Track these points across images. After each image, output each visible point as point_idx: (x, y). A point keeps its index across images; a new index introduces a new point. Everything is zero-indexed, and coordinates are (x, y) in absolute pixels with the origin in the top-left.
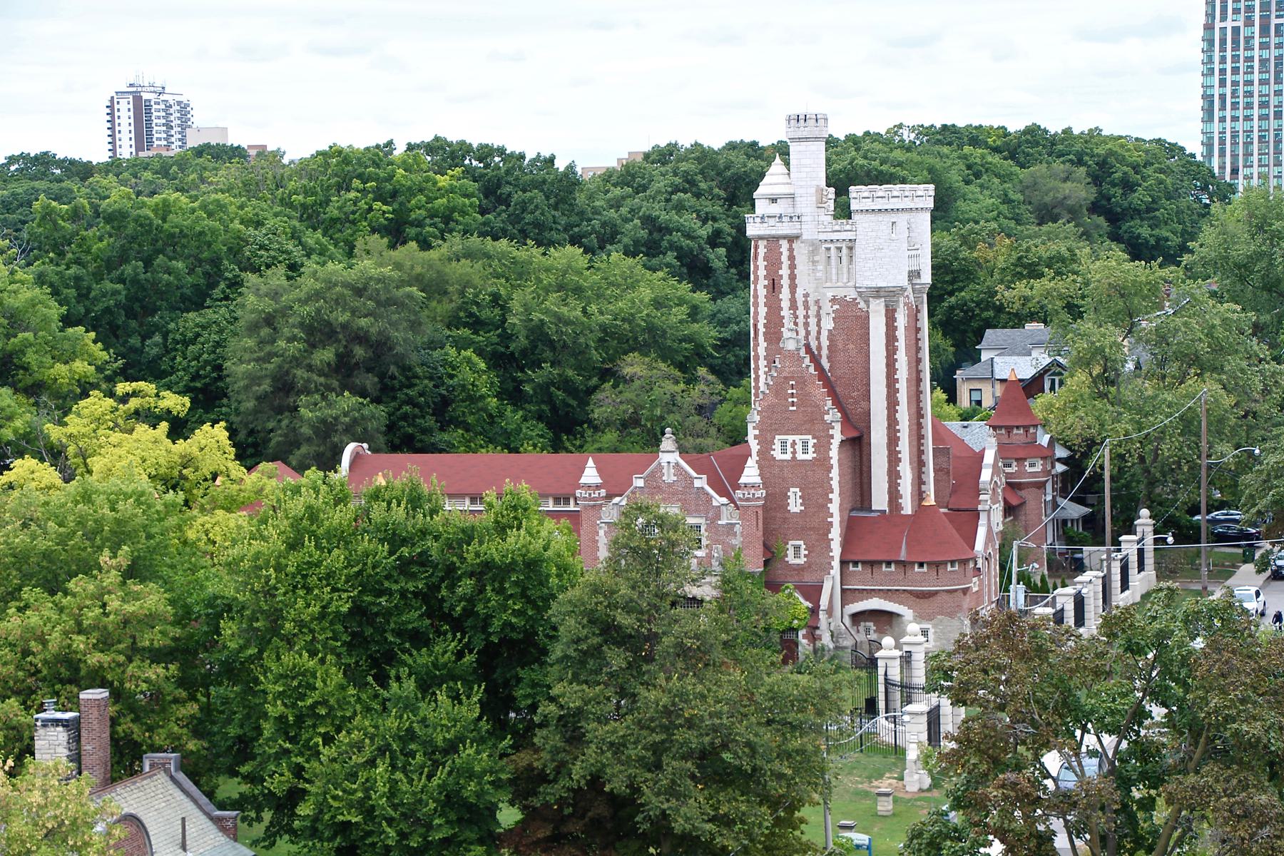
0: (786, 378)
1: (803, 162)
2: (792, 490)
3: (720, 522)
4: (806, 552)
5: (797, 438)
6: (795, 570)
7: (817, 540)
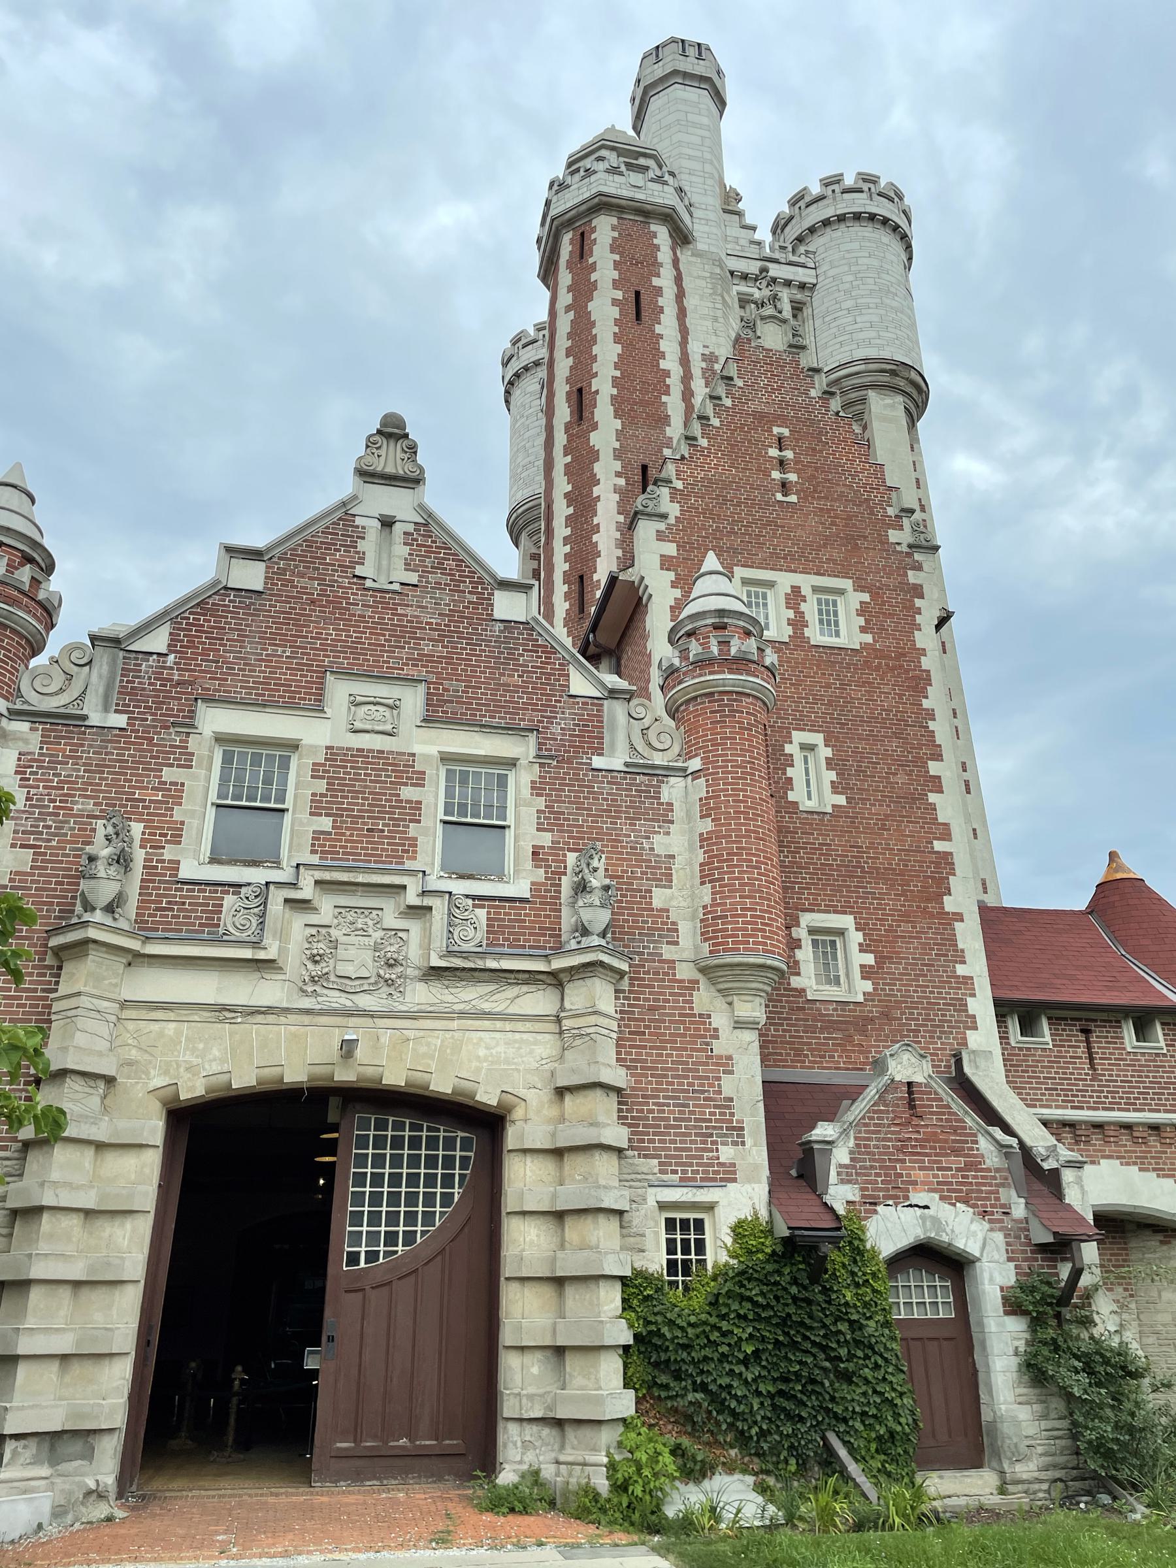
0: (764, 420)
1: (690, 117)
2: (798, 737)
3: (598, 762)
4: (869, 959)
5: (806, 582)
6: (830, 1025)
7: (906, 917)
